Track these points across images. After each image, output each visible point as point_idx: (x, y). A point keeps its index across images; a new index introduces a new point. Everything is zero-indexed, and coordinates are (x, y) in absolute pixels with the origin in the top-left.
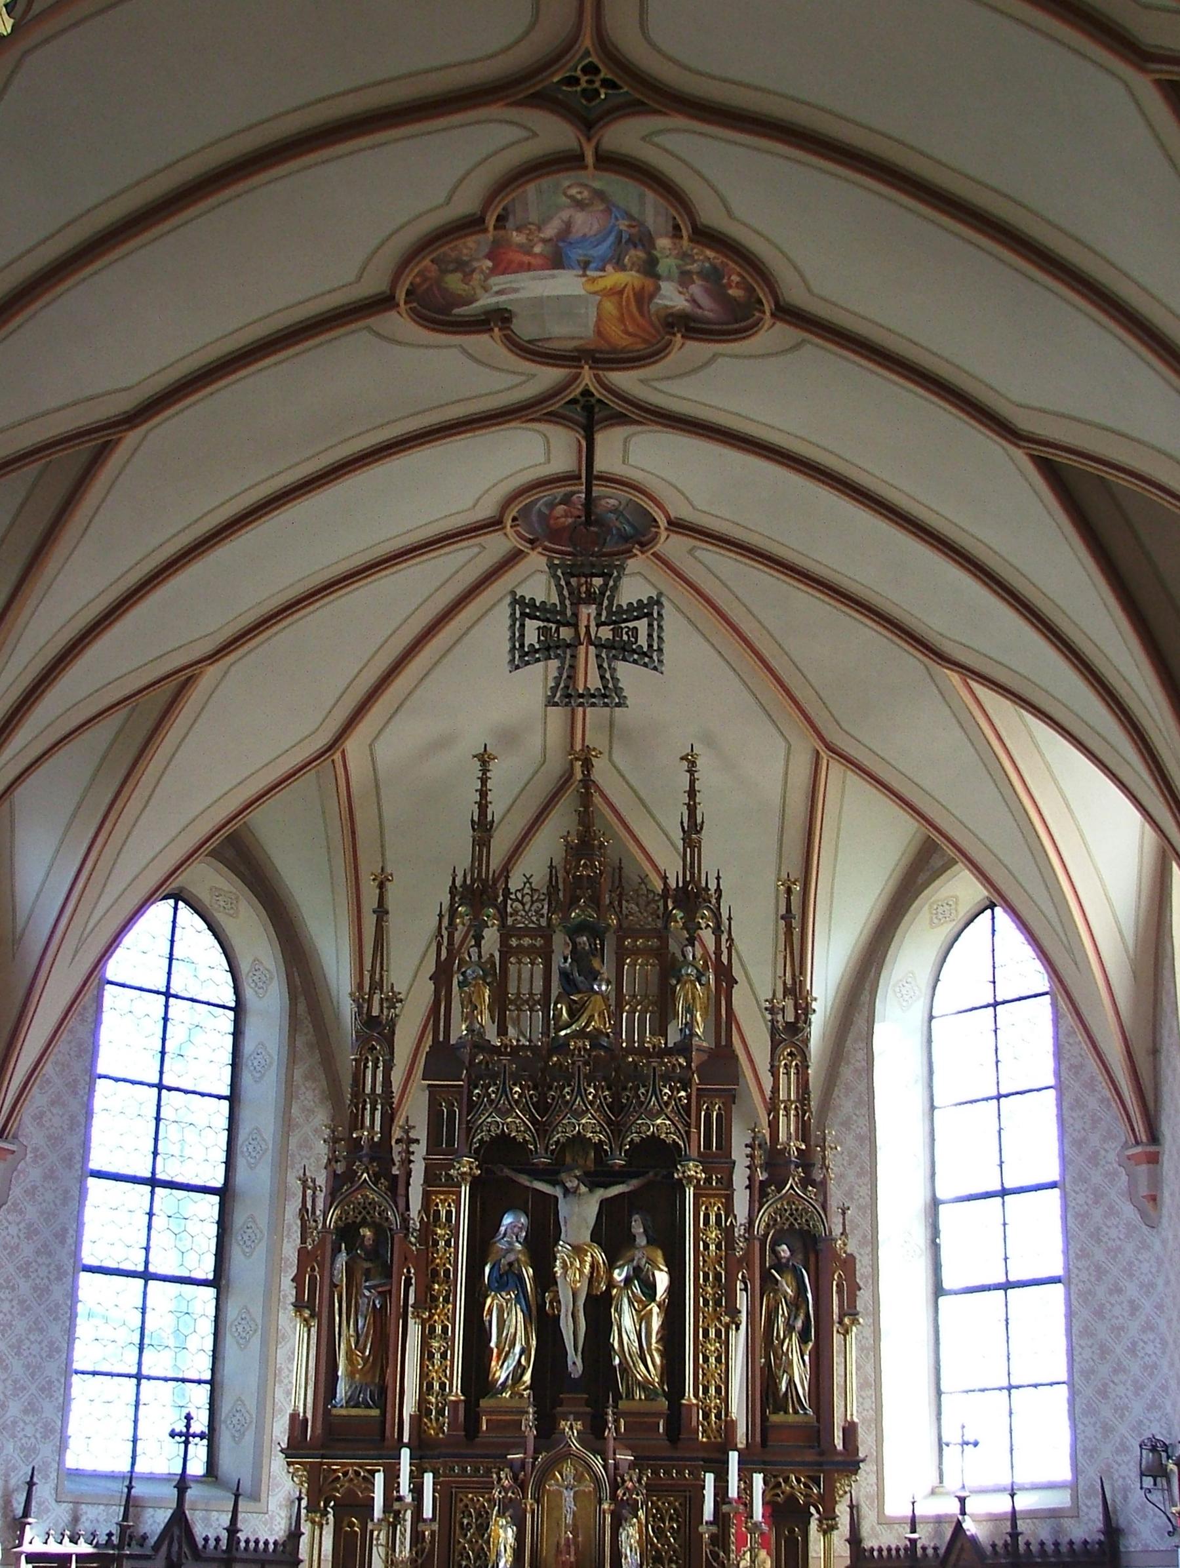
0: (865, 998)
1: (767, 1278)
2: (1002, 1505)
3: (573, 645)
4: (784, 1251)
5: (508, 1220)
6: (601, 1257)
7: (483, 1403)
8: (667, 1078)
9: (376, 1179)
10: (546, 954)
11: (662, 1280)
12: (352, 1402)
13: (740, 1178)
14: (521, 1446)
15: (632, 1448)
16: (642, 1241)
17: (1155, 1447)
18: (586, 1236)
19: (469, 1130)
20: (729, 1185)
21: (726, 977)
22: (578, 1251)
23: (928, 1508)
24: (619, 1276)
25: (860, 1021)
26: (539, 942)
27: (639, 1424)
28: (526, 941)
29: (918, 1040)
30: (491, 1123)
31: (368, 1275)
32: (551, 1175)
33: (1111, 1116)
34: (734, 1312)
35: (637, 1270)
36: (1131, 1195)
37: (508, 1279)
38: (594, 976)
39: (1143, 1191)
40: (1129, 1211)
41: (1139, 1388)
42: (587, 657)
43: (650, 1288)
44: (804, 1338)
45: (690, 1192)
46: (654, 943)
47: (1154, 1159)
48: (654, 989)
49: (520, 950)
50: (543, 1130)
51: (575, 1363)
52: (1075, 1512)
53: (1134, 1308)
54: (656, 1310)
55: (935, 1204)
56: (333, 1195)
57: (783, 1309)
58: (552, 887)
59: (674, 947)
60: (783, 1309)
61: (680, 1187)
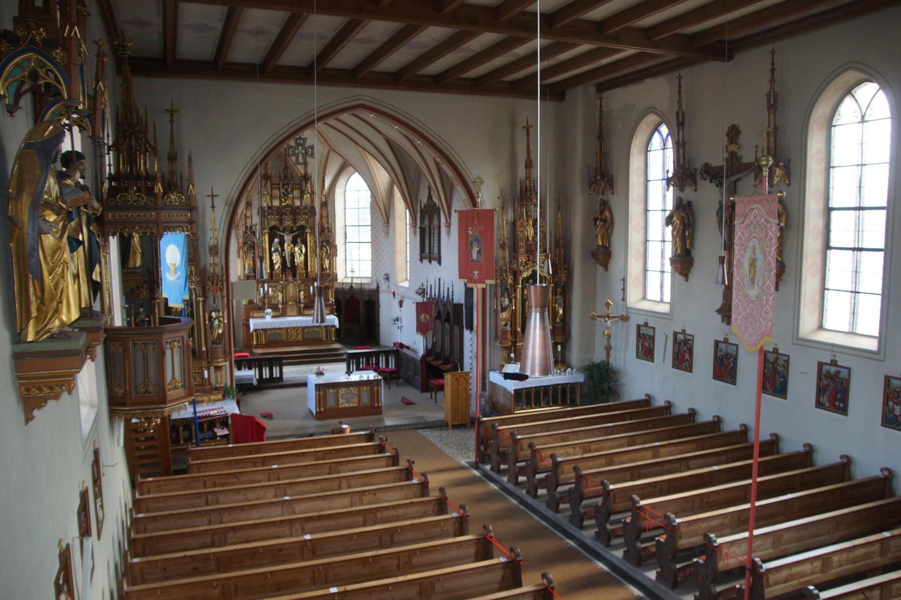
0: (333, 188)
1: (321, 248)
2: (358, 281)
3: (298, 154)
4: (324, 244)
5: (276, 240)
6: (292, 245)
7: (274, 272)
8: (304, 214)
9: (252, 233)
10: (279, 188)
11: (304, 250)
12: (250, 273)
13: (317, 229)
14: (282, 281)
15: (300, 279)
16: (299, 243)
17: (386, 275)
18: (290, 243)
19: (268, 225)
20: (315, 232)
21: (313, 192)
22: (289, 245)
23: (345, 281)
24: (297, 249)
25: (332, 192)
26: (278, 186)
27: (301, 275)
28: (275, 186)
29: (343, 195)
30: (273, 223)
31: (250, 250)
32: (283, 231)
33: (380, 217)
34: (316, 255)
35: (299, 249)
36: (384, 231)
37: (276, 250)
38: (288, 193)
39: (386, 232)
40: (383, 235)
41: (383, 264)
42: (300, 155)
43: (302, 251)
44: (328, 258)
45: (308, 235)
46: (299, 186)
47: (388, 227)
48: (299, 195)
49: (274, 188)
50: (282, 224)
51: (289, 265)
52: (371, 284)
53: (383, 251)
54: (303, 255)
55: (346, 226)
56: (244, 236)
57: (324, 254)
58: (280, 175)
59: (303, 188)
60: (324, 254)
61: (306, 233)
